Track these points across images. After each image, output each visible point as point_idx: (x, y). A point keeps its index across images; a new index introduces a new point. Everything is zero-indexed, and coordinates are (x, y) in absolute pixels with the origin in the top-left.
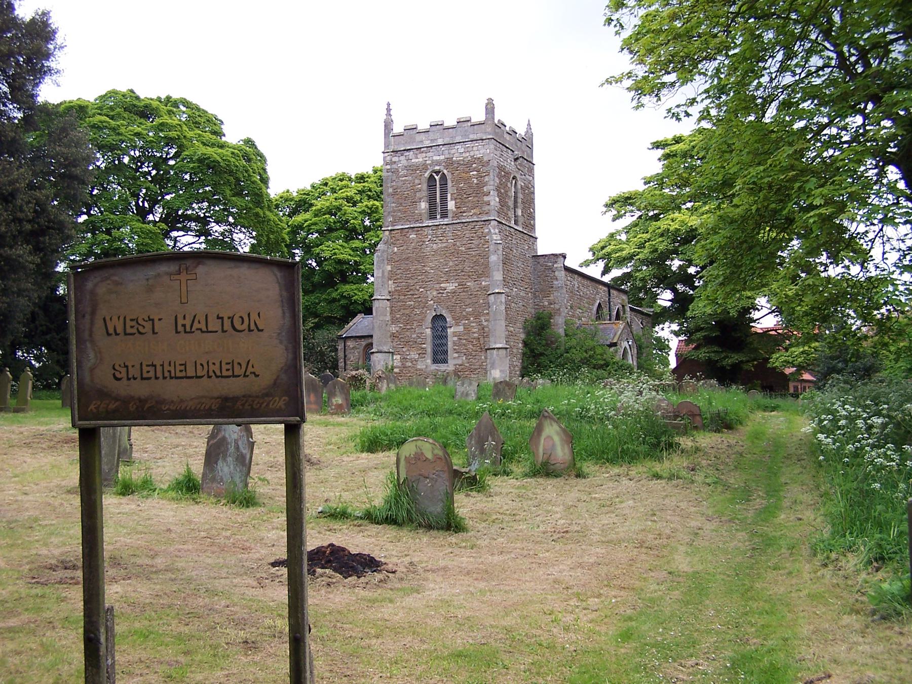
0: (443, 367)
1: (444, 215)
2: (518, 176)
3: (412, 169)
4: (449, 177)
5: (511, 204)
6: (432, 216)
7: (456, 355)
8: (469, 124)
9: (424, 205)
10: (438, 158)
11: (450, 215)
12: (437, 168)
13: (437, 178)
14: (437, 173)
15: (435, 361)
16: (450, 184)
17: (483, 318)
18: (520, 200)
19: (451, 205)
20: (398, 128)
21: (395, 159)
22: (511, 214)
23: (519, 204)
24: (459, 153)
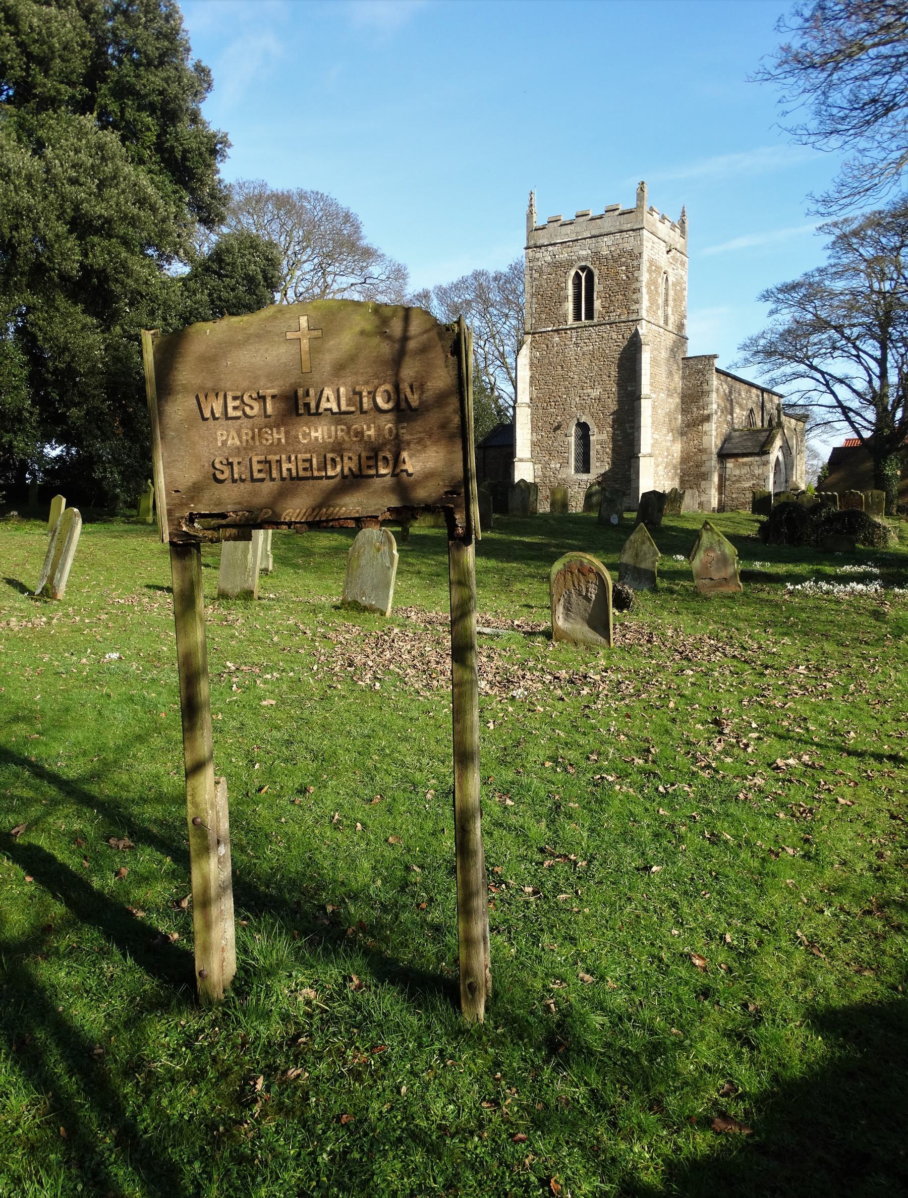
0: (584, 477)
1: (590, 316)
2: (670, 271)
3: (559, 266)
4: (596, 272)
5: (661, 301)
6: (577, 317)
7: (598, 464)
8: (617, 213)
9: (570, 306)
10: (584, 253)
11: (596, 315)
12: (583, 264)
13: (583, 276)
14: (583, 269)
15: (577, 470)
16: (596, 280)
17: (627, 425)
18: (670, 298)
19: (597, 304)
20: (539, 220)
21: (538, 255)
22: (660, 313)
23: (671, 303)
24: (606, 246)
